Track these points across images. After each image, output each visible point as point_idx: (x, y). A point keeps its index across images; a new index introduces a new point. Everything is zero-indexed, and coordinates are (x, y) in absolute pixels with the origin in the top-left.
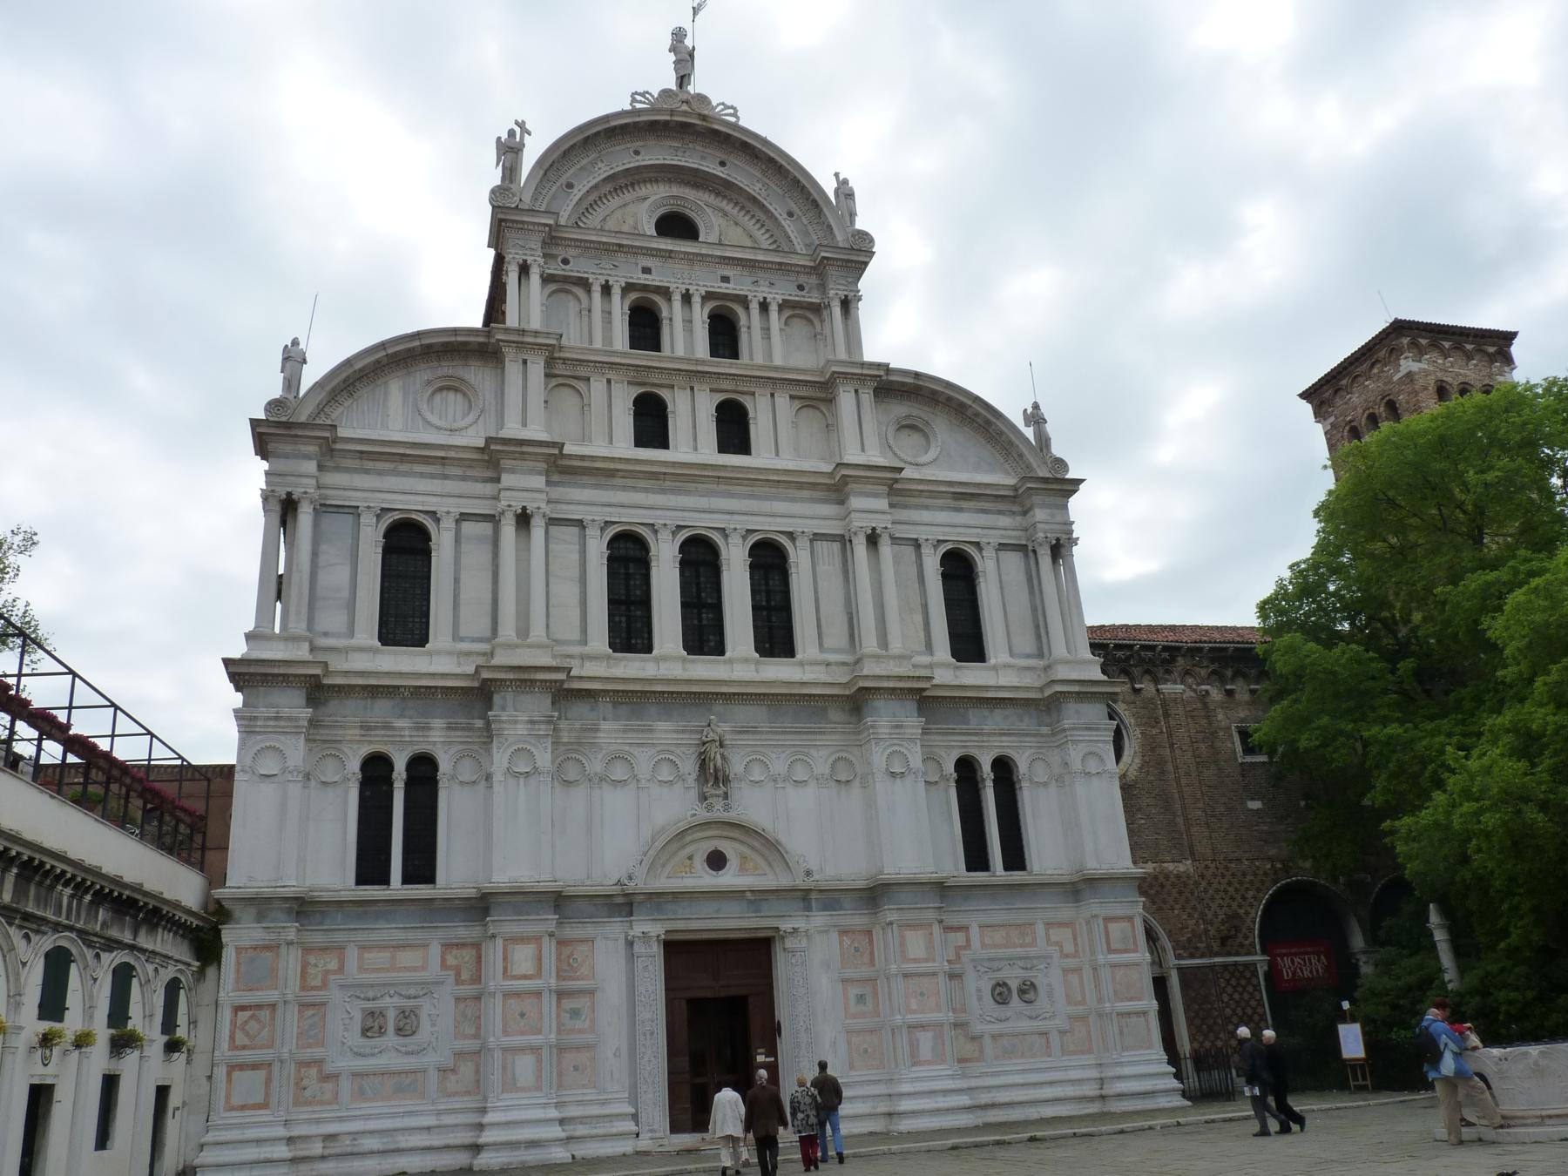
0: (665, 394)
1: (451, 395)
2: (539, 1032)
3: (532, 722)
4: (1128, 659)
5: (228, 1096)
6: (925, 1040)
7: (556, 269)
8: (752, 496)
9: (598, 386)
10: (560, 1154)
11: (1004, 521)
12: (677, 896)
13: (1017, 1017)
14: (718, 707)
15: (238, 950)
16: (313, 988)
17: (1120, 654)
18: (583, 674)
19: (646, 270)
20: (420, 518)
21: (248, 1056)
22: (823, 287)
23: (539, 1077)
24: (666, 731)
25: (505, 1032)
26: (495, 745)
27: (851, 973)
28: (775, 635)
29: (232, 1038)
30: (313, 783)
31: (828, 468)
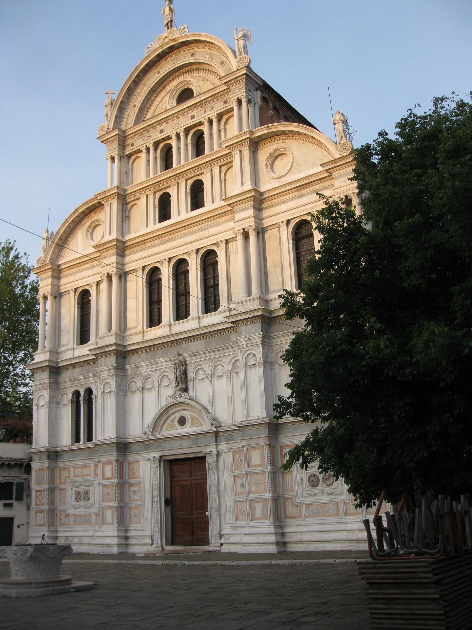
3: (108, 370)
5: (36, 521)
6: (259, 507)
7: (128, 151)
8: (201, 230)
12: (165, 439)
14: (185, 345)
15: (36, 471)
16: (63, 483)
20: (86, 287)
21: (40, 508)
23: (113, 519)
24: (164, 362)
27: (237, 473)
29: (36, 502)
30: (61, 406)
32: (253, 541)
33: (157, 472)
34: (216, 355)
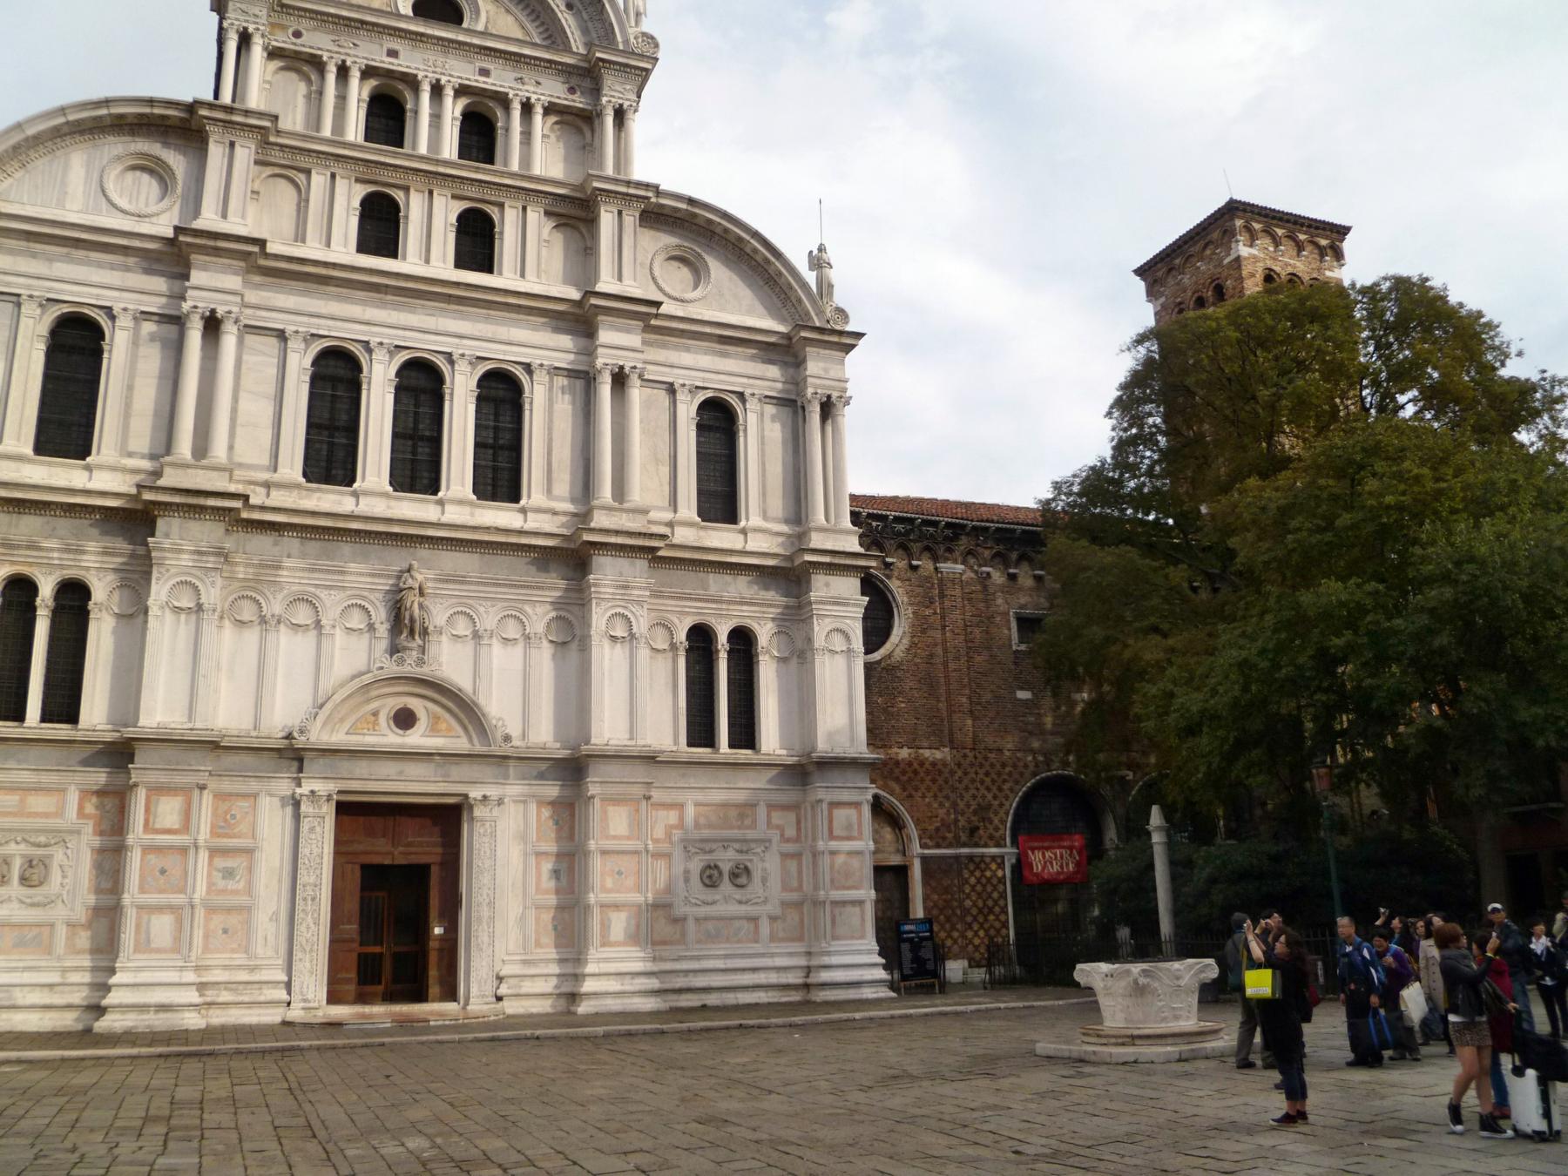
0: (399, 196)
1: (145, 177)
2: (183, 890)
4: (907, 533)
7: (283, 40)
9: (319, 180)
10: (193, 1020)
11: (773, 371)
13: (726, 901)
14: (424, 552)
17: (900, 527)
18: (268, 503)
19: (393, 53)
22: (596, 92)
25: (142, 890)
26: (155, 574)
28: (500, 475)
31: (575, 295)
32: (611, 989)
33: (318, 829)
34: (512, 594)
